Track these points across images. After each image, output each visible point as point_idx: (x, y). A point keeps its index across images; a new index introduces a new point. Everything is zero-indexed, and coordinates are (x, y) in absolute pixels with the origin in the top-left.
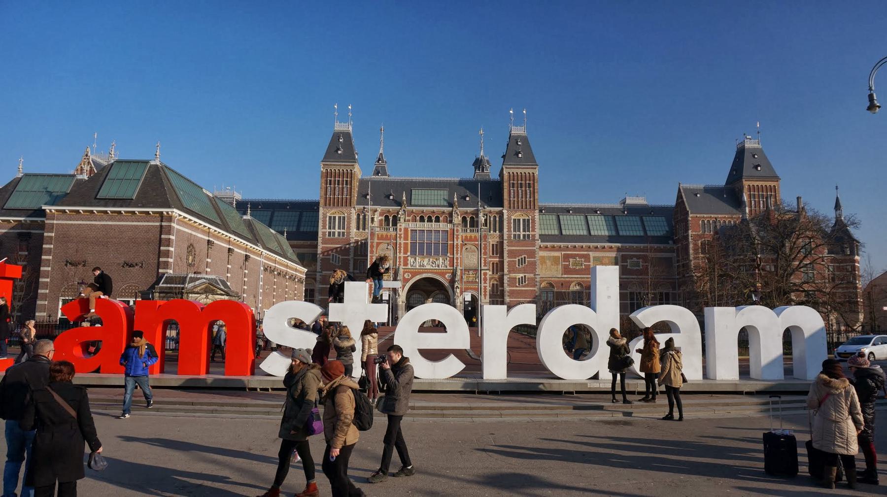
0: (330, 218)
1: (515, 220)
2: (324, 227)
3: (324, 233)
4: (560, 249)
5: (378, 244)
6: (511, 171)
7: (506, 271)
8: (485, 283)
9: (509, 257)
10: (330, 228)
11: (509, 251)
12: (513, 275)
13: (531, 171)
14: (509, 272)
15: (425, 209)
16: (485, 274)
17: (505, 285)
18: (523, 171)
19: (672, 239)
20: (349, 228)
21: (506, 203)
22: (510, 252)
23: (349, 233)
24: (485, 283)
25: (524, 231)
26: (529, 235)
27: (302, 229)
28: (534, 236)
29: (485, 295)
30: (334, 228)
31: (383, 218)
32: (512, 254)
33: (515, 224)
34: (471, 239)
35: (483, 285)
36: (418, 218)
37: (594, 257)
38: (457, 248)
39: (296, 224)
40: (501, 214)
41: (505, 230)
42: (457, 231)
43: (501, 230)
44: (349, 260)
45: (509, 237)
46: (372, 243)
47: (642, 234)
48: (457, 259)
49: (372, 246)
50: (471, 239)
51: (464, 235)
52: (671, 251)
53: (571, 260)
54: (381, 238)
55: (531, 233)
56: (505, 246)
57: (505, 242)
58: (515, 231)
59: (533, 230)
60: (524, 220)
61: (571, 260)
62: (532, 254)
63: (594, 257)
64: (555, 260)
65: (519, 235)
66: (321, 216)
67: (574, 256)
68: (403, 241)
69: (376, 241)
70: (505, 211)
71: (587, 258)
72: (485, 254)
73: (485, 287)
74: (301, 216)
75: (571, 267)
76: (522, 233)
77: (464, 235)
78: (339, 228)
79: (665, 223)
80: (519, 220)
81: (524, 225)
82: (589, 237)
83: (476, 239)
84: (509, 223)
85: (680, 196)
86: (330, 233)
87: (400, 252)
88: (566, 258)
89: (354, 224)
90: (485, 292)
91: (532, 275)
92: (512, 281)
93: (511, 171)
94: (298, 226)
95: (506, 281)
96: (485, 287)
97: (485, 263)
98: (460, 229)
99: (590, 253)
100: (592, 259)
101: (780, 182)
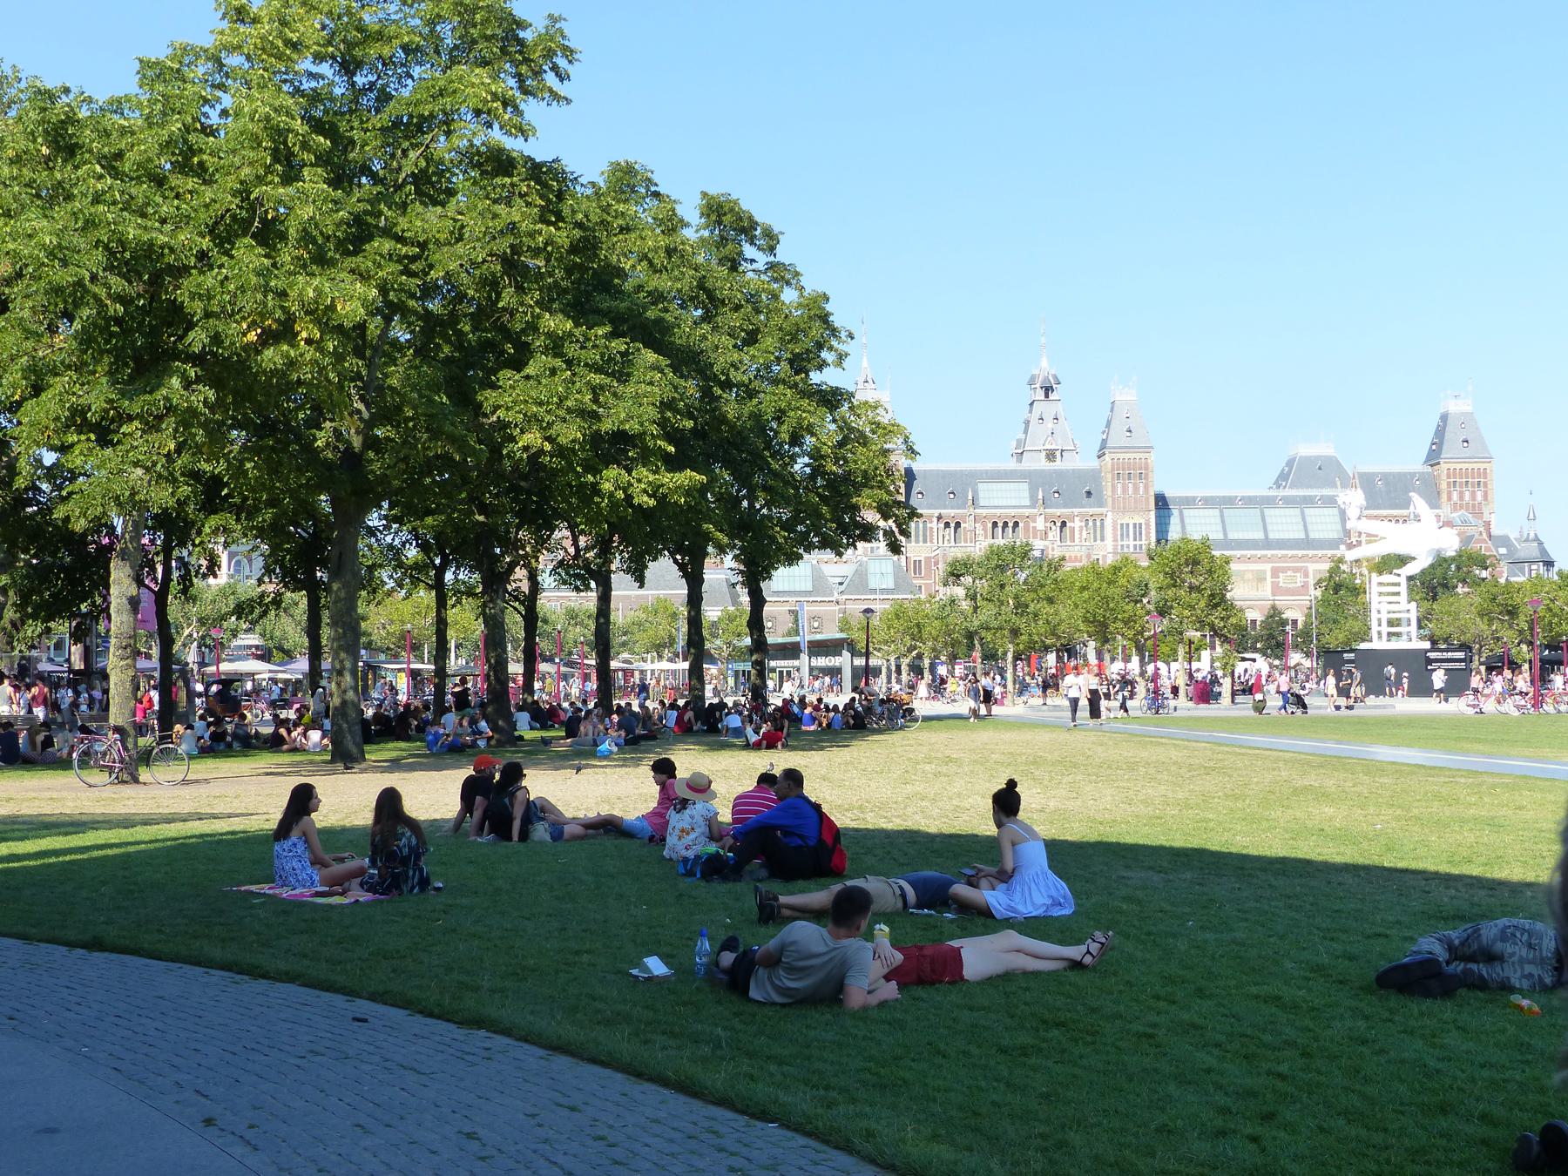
13: (1143, 456)
18: (1132, 456)
43: (1102, 539)
45: (1115, 547)
76: (1132, 543)
84: (1115, 529)
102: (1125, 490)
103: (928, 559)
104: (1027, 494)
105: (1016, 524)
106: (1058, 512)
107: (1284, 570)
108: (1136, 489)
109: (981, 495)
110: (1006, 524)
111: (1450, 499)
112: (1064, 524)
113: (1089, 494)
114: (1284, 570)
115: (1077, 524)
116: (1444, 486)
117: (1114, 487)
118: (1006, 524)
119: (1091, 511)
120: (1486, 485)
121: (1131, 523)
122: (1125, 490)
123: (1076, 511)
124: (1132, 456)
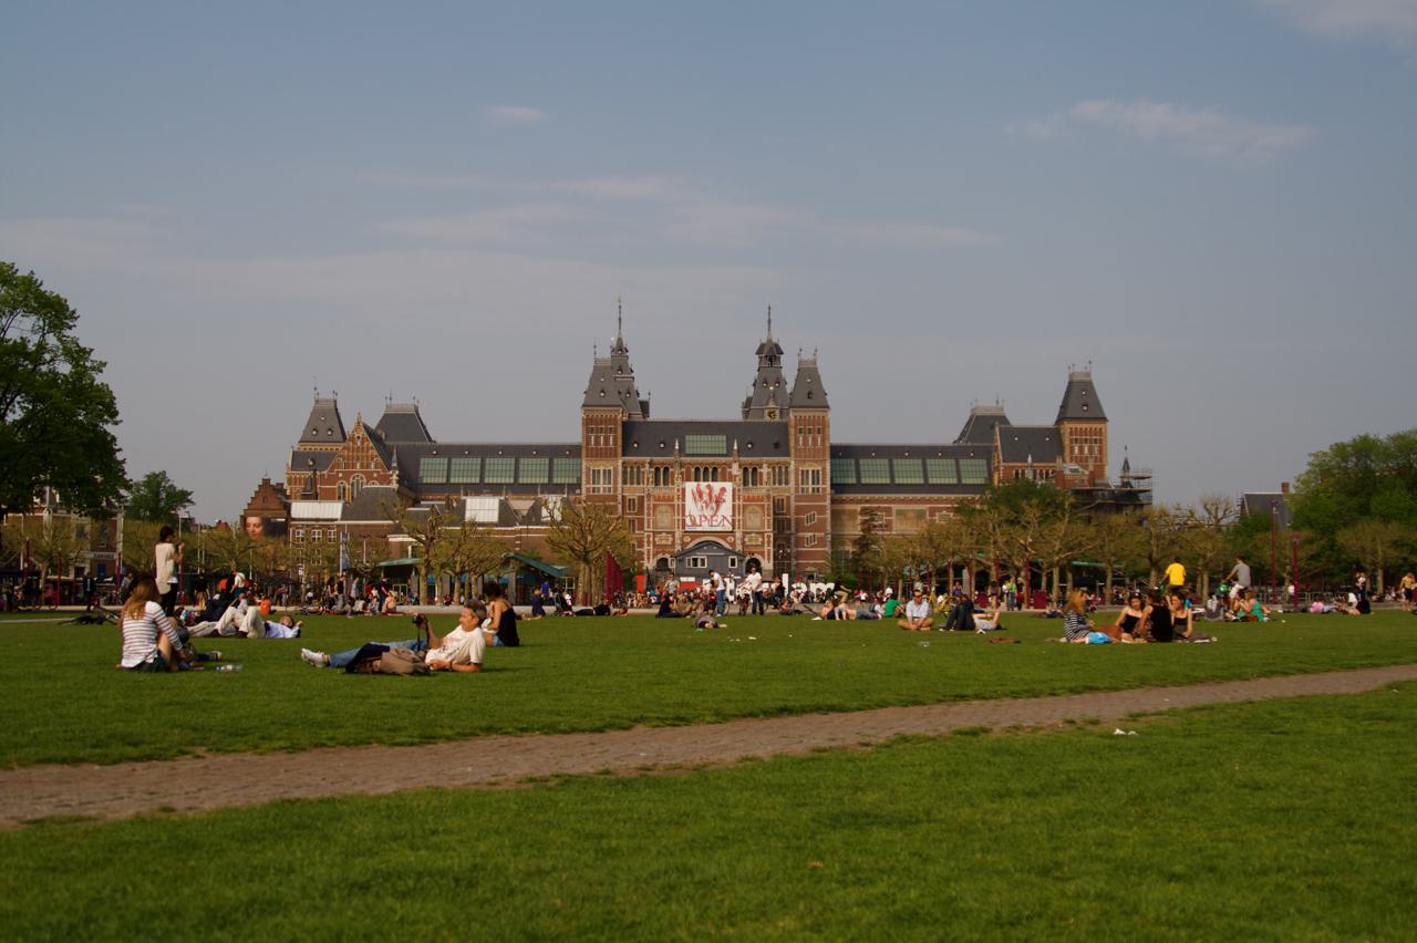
0: (594, 471)
1: (803, 471)
2: (588, 482)
3: (588, 489)
6: (798, 414)
7: (793, 529)
10: (594, 483)
12: (801, 534)
13: (821, 414)
14: (797, 530)
15: (700, 459)
16: (769, 537)
17: (792, 546)
18: (812, 414)
20: (616, 483)
21: (793, 451)
23: (616, 489)
25: (813, 483)
26: (818, 489)
28: (824, 489)
29: (769, 559)
35: (766, 548)
36: (693, 470)
41: (792, 483)
42: (739, 490)
43: (787, 483)
46: (649, 505)
50: (753, 500)
54: (658, 499)
55: (820, 486)
57: (792, 497)
60: (813, 472)
64: (853, 514)
65: (808, 489)
66: (584, 470)
69: (652, 502)
70: (793, 462)
71: (888, 511)
72: (768, 515)
74: (551, 464)
76: (810, 486)
80: (807, 471)
81: (813, 478)
82: (893, 487)
83: (759, 499)
84: (797, 474)
86: (594, 489)
90: (769, 555)
93: (798, 414)
95: (793, 541)
97: (769, 525)
100: (894, 512)
101: (1108, 424)
102: (805, 440)
104: (725, 445)
105: (715, 469)
106: (750, 459)
107: (940, 510)
110: (706, 469)
111: (1072, 451)
113: (777, 445)
114: (940, 510)
115: (765, 470)
116: (1067, 442)
117: (797, 441)
118: (706, 469)
119: (777, 459)
120: (1101, 441)
121: (810, 470)
122: (805, 440)
123: (765, 459)
124: (812, 414)
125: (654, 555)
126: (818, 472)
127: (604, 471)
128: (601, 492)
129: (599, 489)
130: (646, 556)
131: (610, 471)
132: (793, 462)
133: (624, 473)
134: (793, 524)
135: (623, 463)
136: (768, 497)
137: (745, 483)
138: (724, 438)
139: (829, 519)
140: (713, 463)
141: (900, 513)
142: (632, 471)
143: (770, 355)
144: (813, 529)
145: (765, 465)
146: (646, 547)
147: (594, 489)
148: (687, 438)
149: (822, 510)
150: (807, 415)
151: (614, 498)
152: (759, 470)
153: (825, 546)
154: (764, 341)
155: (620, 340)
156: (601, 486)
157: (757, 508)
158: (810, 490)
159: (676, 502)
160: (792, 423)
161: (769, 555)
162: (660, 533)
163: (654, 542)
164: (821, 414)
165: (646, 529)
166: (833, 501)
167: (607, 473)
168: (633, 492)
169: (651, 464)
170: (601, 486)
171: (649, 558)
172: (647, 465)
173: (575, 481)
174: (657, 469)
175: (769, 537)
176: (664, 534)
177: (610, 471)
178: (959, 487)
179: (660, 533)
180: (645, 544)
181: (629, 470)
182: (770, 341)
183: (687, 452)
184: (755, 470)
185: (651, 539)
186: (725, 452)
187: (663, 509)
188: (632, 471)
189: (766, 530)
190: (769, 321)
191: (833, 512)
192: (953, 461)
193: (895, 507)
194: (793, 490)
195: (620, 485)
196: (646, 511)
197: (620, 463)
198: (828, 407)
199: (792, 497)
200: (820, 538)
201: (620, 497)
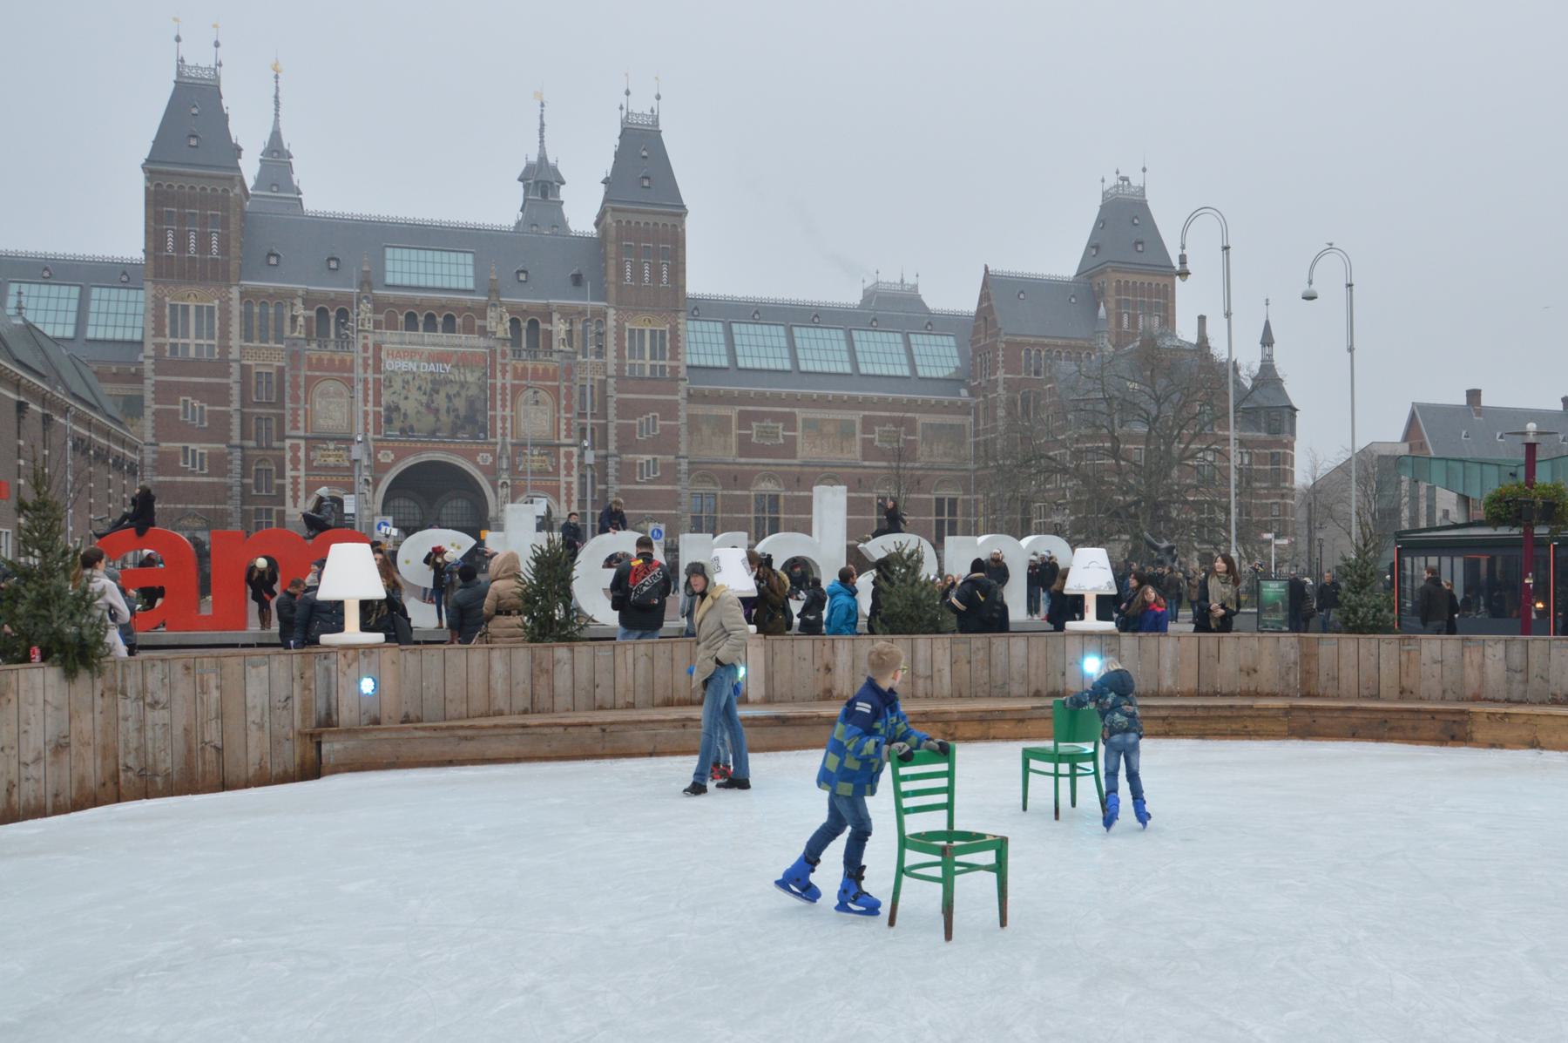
0: (174, 308)
2: (159, 331)
3: (159, 348)
4: (729, 400)
5: (310, 381)
7: (612, 447)
8: (569, 474)
9: (619, 416)
10: (174, 334)
11: (621, 404)
13: (669, 221)
14: (622, 448)
16: (569, 455)
17: (611, 479)
18: (651, 219)
19: (967, 386)
20: (225, 335)
21: (612, 290)
22: (621, 404)
23: (225, 349)
24: (569, 474)
25: (653, 357)
27: (91, 333)
28: (675, 369)
30: (186, 335)
31: (313, 314)
32: (625, 409)
33: (631, 337)
34: (535, 375)
35: (563, 479)
36: (402, 318)
37: (805, 420)
38: (504, 393)
39: (72, 318)
40: (600, 317)
42: (504, 355)
43: (600, 351)
44: (228, 415)
45: (620, 367)
47: (906, 372)
48: (504, 419)
49: (295, 386)
51: (520, 365)
52: (964, 409)
53: (754, 424)
54: (319, 365)
56: (611, 391)
57: (611, 381)
58: (632, 357)
59: (674, 356)
60: (653, 332)
61: (754, 424)
62: (670, 411)
63: (805, 420)
64: (722, 425)
67: (760, 417)
68: (370, 376)
69: (304, 372)
70: (611, 312)
71: (789, 421)
72: (569, 409)
73: (569, 484)
75: (754, 440)
76: (648, 362)
77: (520, 365)
78: (198, 336)
79: (955, 353)
80: (642, 332)
81: (653, 348)
83: (546, 375)
85: (985, 296)
87: (366, 401)
88: (745, 419)
89: (235, 328)
90: (569, 495)
91: (671, 458)
92: (627, 473)
93: (624, 218)
94: (81, 323)
95: (611, 471)
96: (569, 484)
97: (568, 430)
98: (508, 350)
99: (796, 410)
100: (800, 424)
102: (637, 273)
103: (281, 370)
104: (470, 271)
108: (656, 274)
109: (389, 265)
112: (533, 324)
113: (577, 280)
115: (559, 328)
118: (430, 318)
121: (648, 329)
122: (637, 273)
124: (651, 219)
125: (310, 488)
126: (663, 333)
127: (199, 309)
128: (192, 353)
129: (186, 346)
130: (289, 493)
131: (211, 309)
132: (611, 312)
133: (247, 317)
134: (612, 436)
135: (243, 295)
136: (569, 371)
137: (515, 341)
138: (469, 258)
139: (684, 430)
140: (443, 307)
141: (809, 424)
142: (264, 316)
143: (541, 183)
144: (655, 446)
145: (556, 317)
146: (289, 473)
147: (174, 347)
148: (389, 252)
149: (670, 411)
150: (642, 219)
151: (222, 367)
152: (542, 326)
153: (677, 481)
154: (534, 159)
155: (276, 136)
156: (192, 341)
157: (542, 395)
158: (647, 373)
159: (359, 372)
160: (612, 232)
161: (569, 495)
162: (324, 440)
163: (308, 461)
164: (669, 221)
165: (288, 431)
166: (692, 397)
167: (204, 313)
168: (268, 357)
169: (308, 303)
170: (192, 341)
171: (295, 498)
172: (299, 302)
173: (138, 337)
174: (322, 313)
175: (569, 455)
176: (332, 446)
177: (211, 309)
178: (913, 380)
179: (324, 440)
180: (288, 466)
181: (256, 310)
182: (543, 158)
183: (389, 281)
184: (533, 324)
185: (302, 454)
186: (471, 285)
187: (331, 386)
188: (264, 316)
189: (564, 440)
190: (542, 125)
191: (691, 417)
192: (899, 337)
193: (801, 414)
194: (611, 370)
195: (236, 342)
196: (288, 390)
197: (235, 293)
198: (683, 207)
199: (611, 381)
200: (665, 467)
201: (235, 369)
